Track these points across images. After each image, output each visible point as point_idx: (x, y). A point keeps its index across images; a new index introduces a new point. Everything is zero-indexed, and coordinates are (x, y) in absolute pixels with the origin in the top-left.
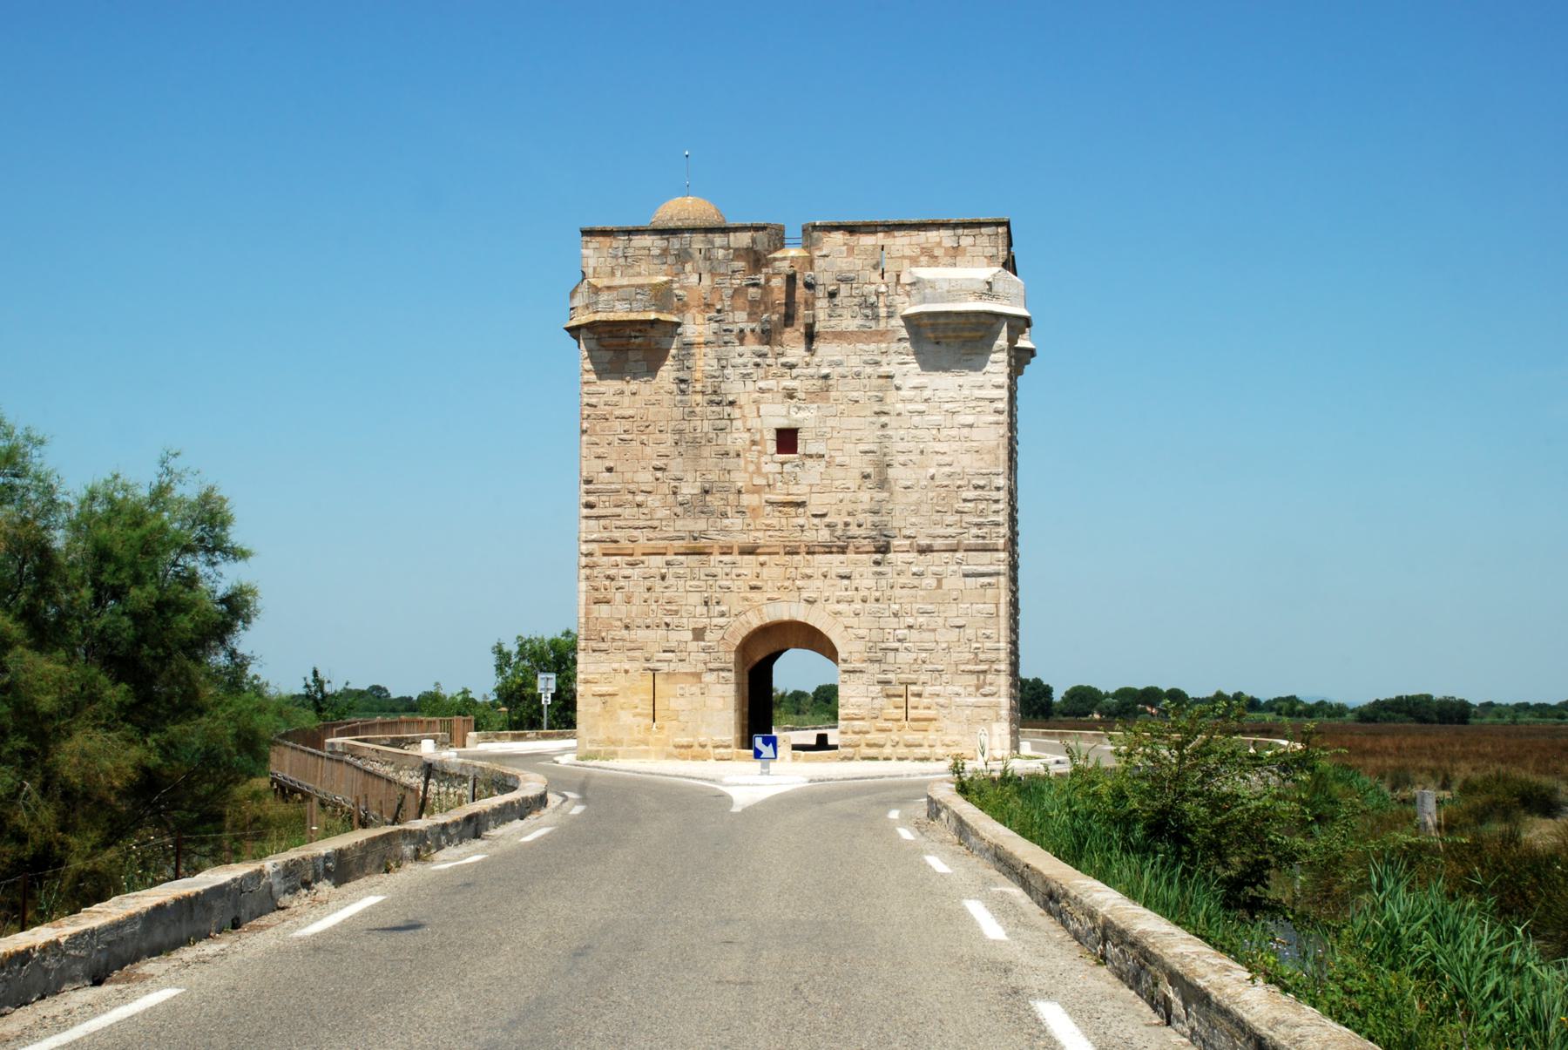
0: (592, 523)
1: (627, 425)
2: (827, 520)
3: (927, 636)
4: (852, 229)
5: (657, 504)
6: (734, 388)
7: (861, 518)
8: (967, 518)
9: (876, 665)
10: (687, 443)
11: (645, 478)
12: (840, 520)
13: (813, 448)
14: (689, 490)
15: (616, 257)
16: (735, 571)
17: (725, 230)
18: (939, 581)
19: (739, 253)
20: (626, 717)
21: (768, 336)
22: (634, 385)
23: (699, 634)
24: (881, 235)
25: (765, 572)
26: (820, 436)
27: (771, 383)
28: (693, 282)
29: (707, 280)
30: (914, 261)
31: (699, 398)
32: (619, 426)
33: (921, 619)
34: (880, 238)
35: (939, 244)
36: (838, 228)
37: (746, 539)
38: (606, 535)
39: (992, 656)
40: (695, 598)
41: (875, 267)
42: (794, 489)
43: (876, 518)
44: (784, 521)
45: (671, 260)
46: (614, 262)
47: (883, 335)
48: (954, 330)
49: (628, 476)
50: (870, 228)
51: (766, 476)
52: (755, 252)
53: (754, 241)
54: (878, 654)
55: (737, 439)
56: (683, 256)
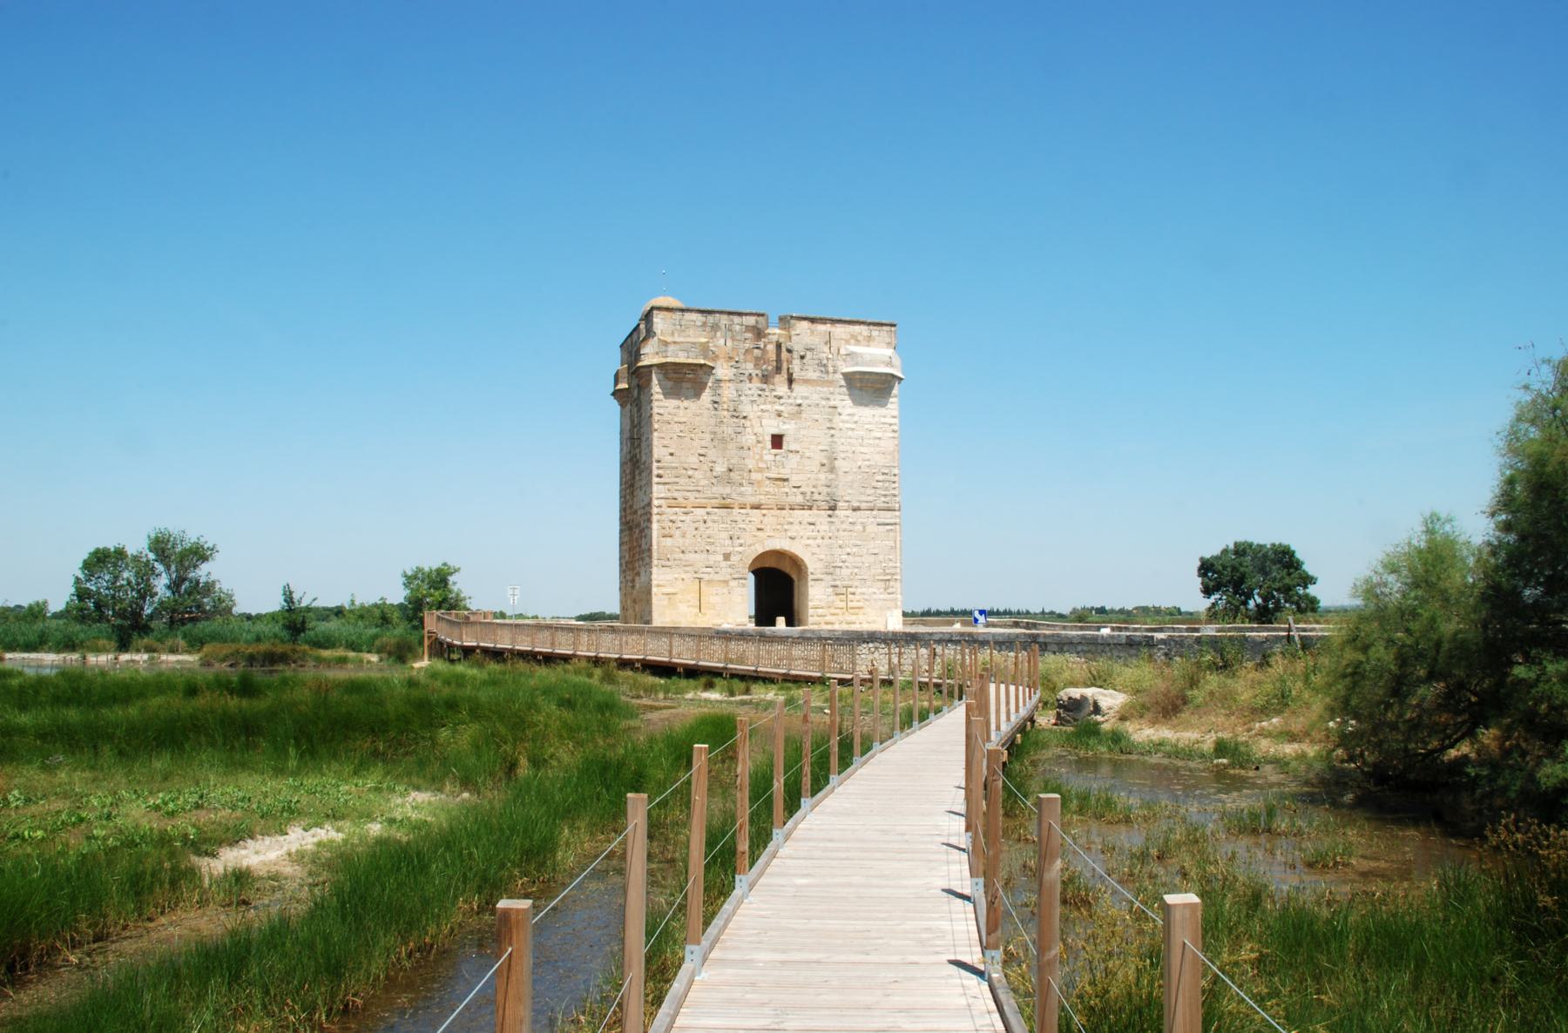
1: (682, 427)
4: (813, 320)
6: (746, 409)
10: (719, 440)
11: (693, 460)
12: (808, 490)
13: (793, 447)
14: (720, 469)
17: (740, 314)
19: (748, 328)
20: (683, 608)
21: (765, 379)
22: (686, 403)
23: (727, 557)
25: (766, 520)
26: (796, 440)
27: (768, 407)
28: (720, 343)
29: (729, 343)
30: (847, 342)
32: (677, 428)
34: (828, 327)
37: (754, 500)
40: (725, 535)
47: (831, 383)
50: (823, 321)
54: (831, 569)
55: (748, 439)
56: (715, 328)
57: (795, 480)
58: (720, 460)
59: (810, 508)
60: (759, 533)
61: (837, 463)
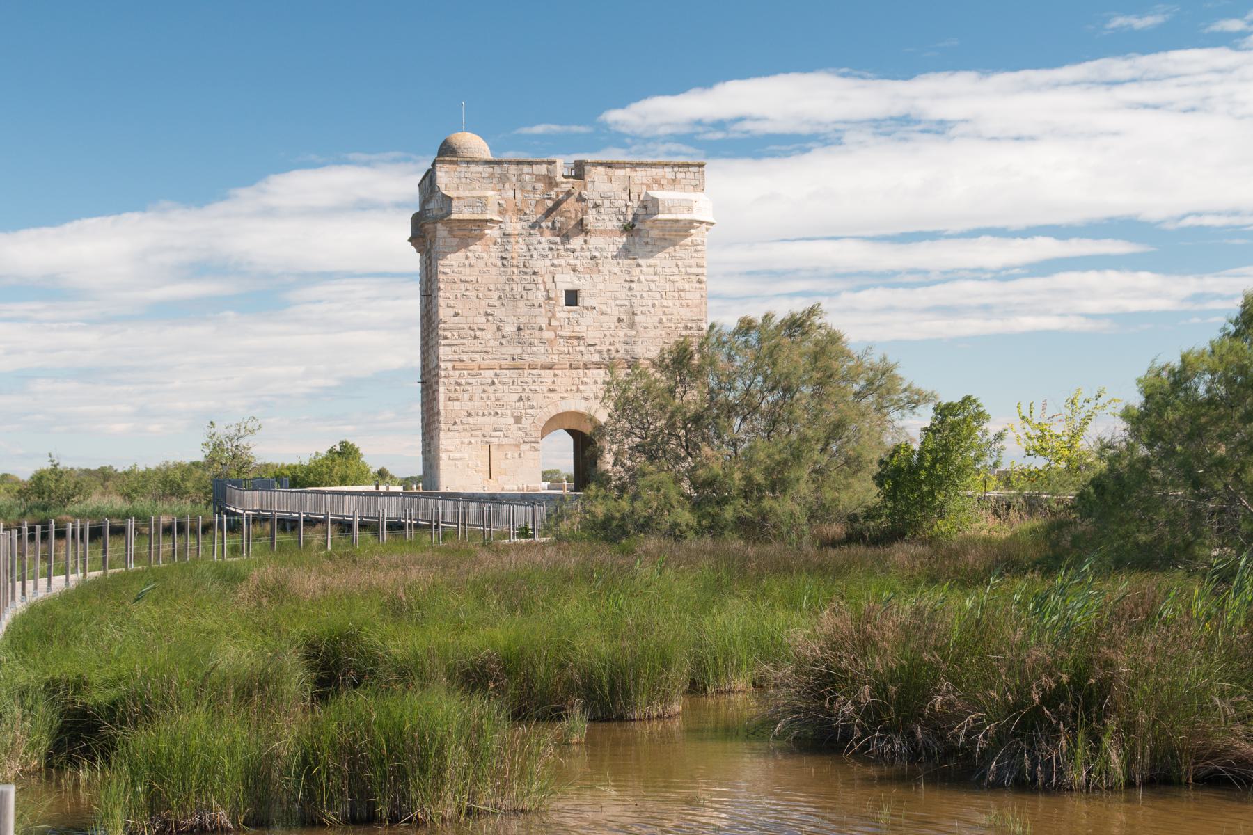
4: (610, 165)
6: (538, 264)
7: (618, 346)
10: (507, 297)
13: (587, 304)
14: (509, 328)
17: (530, 163)
19: (539, 178)
23: (518, 420)
25: (558, 380)
31: (515, 270)
34: (628, 171)
35: (664, 177)
36: (601, 164)
38: (456, 357)
41: (625, 190)
42: (577, 328)
43: (628, 347)
45: (495, 181)
49: (470, 319)
56: (503, 179)
57: (591, 337)
58: (510, 319)
60: (551, 395)
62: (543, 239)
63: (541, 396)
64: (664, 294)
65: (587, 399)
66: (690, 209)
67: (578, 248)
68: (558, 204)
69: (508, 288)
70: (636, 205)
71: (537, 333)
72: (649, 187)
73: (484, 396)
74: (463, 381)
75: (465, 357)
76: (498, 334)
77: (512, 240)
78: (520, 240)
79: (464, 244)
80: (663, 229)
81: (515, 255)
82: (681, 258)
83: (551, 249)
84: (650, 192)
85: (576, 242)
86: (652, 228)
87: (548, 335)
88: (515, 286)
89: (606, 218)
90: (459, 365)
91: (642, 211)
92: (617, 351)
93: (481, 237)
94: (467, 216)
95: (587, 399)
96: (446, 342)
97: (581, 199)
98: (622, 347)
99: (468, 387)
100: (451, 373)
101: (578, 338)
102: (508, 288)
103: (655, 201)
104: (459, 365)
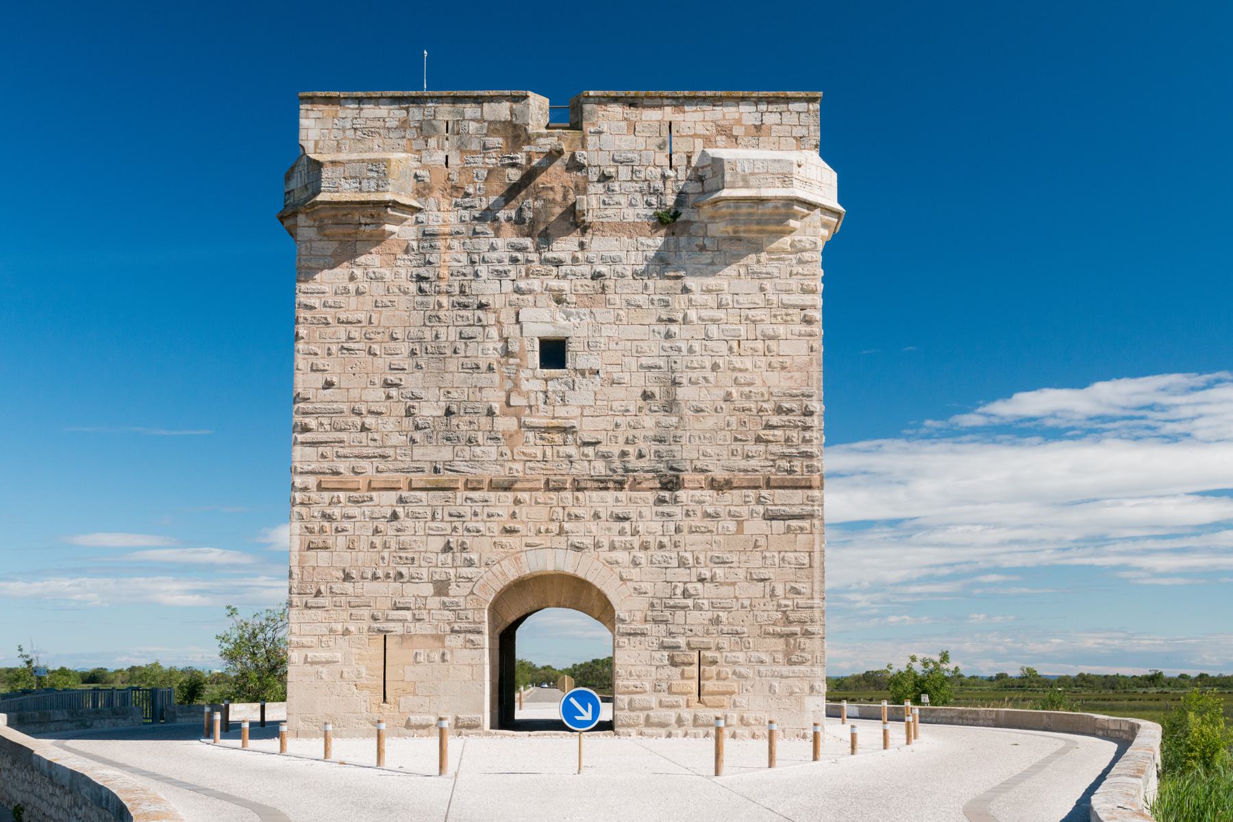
0: (308, 450)
2: (601, 448)
3: (725, 591)
4: (632, 103)
5: (390, 427)
6: (488, 289)
8: (773, 448)
9: (663, 627)
10: (428, 353)
13: (582, 363)
14: (429, 410)
15: (344, 130)
16: (486, 510)
18: (740, 524)
19: (495, 127)
23: (441, 588)
24: (668, 109)
25: (522, 512)
31: (444, 300)
32: (342, 332)
33: (720, 572)
34: (668, 113)
35: (739, 122)
36: (616, 100)
38: (325, 465)
39: (804, 615)
41: (661, 147)
42: (561, 411)
44: (549, 451)
45: (410, 133)
46: (340, 135)
48: (759, 223)
49: (355, 394)
51: (527, 395)
52: (515, 126)
53: (512, 113)
54: (663, 610)
59: (620, 485)
61: (681, 393)
62: (499, 242)
63: (487, 542)
64: (735, 344)
65: (577, 548)
66: (786, 179)
67: (567, 257)
68: (530, 175)
69: (428, 335)
70: (682, 175)
71: (484, 421)
72: (708, 141)
73: (377, 540)
74: (336, 511)
75: (342, 466)
76: (407, 423)
77: (440, 243)
78: (455, 243)
79: (348, 251)
80: (733, 219)
81: (444, 272)
82: (770, 276)
83: (514, 261)
84: (709, 151)
85: (564, 247)
86: (713, 218)
87: (506, 424)
88: (442, 331)
89: (623, 200)
90: (329, 480)
91: (694, 187)
92: (641, 456)
93: (380, 239)
94: (348, 194)
95: (577, 548)
96: (308, 436)
97: (575, 166)
98: (649, 448)
99: (347, 525)
100: (314, 495)
101: (564, 430)
102: (428, 335)
103: (718, 163)
104: (329, 480)
